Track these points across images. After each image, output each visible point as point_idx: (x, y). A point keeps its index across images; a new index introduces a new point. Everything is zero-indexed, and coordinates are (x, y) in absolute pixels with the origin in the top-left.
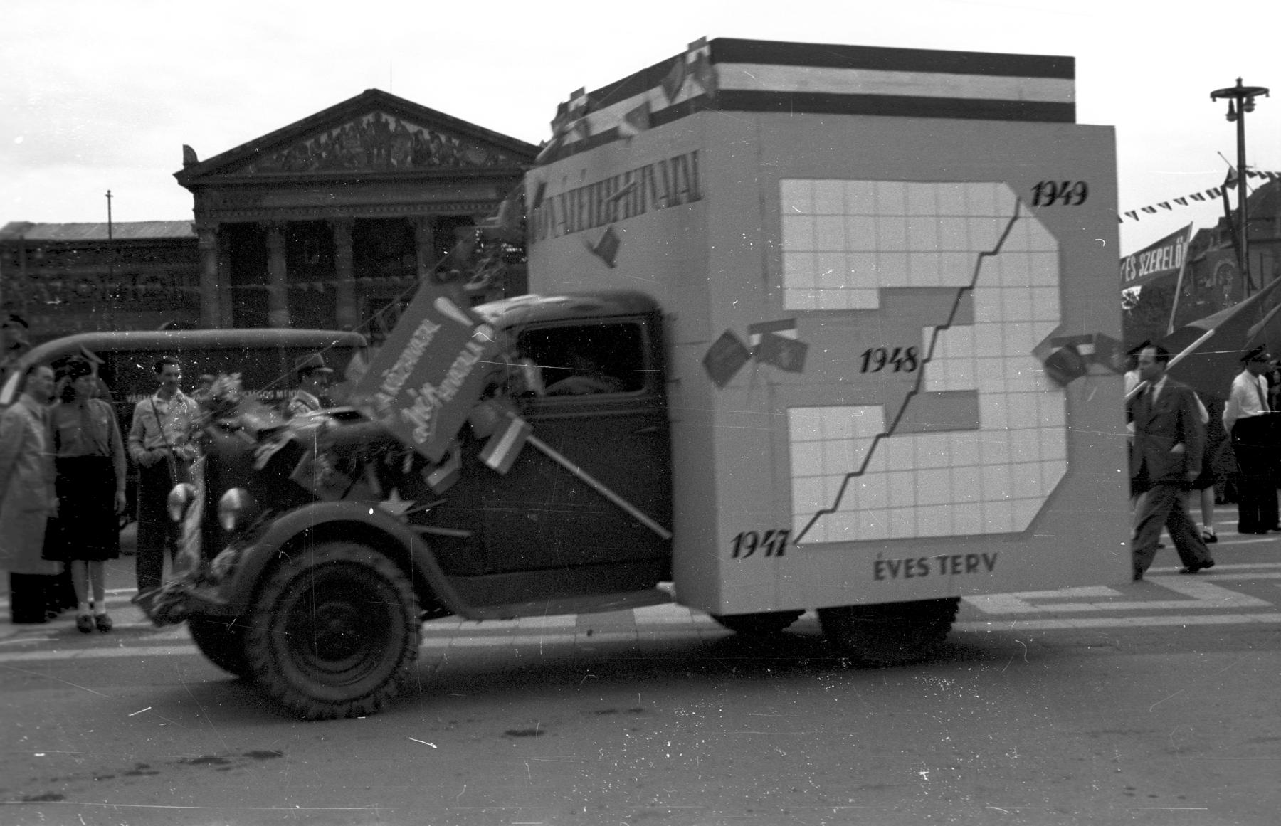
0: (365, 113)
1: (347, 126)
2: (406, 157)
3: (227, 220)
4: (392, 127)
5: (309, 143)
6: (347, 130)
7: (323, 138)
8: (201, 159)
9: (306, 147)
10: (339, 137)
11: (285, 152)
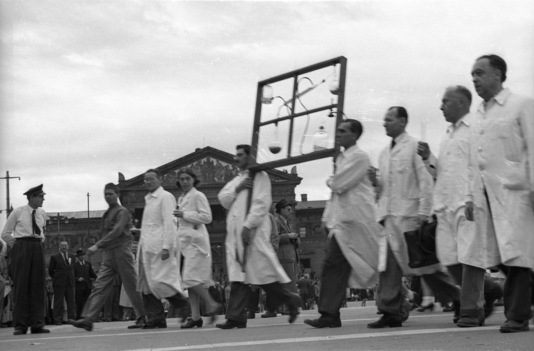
0: (203, 158)
1: (194, 164)
3: (139, 207)
4: (215, 164)
6: (194, 165)
8: (126, 179)
9: (175, 173)
11: (165, 176)
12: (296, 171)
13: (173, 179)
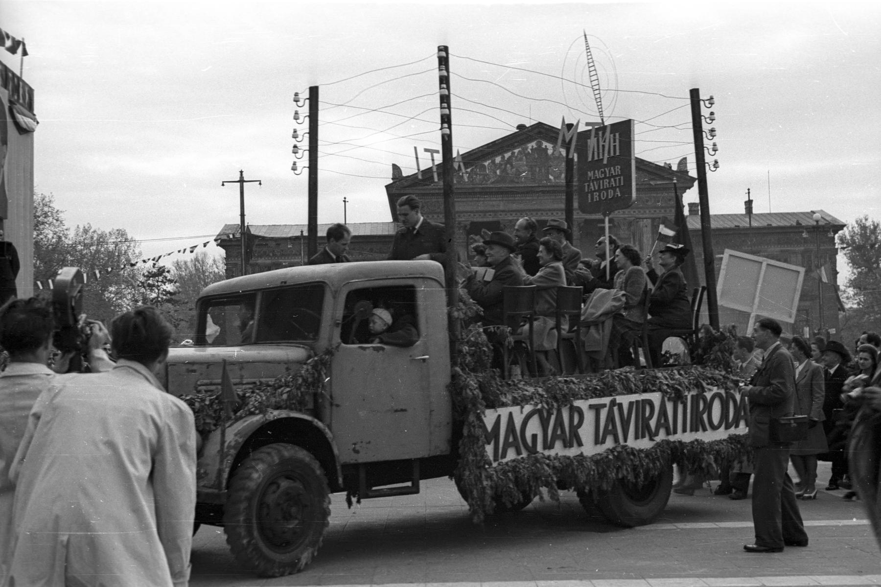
0: (530, 141)
1: (516, 151)
2: (561, 174)
4: (550, 152)
5: (486, 164)
6: (516, 154)
7: (498, 160)
8: (404, 174)
9: (484, 165)
10: (510, 158)
12: (686, 166)
13: (481, 177)
